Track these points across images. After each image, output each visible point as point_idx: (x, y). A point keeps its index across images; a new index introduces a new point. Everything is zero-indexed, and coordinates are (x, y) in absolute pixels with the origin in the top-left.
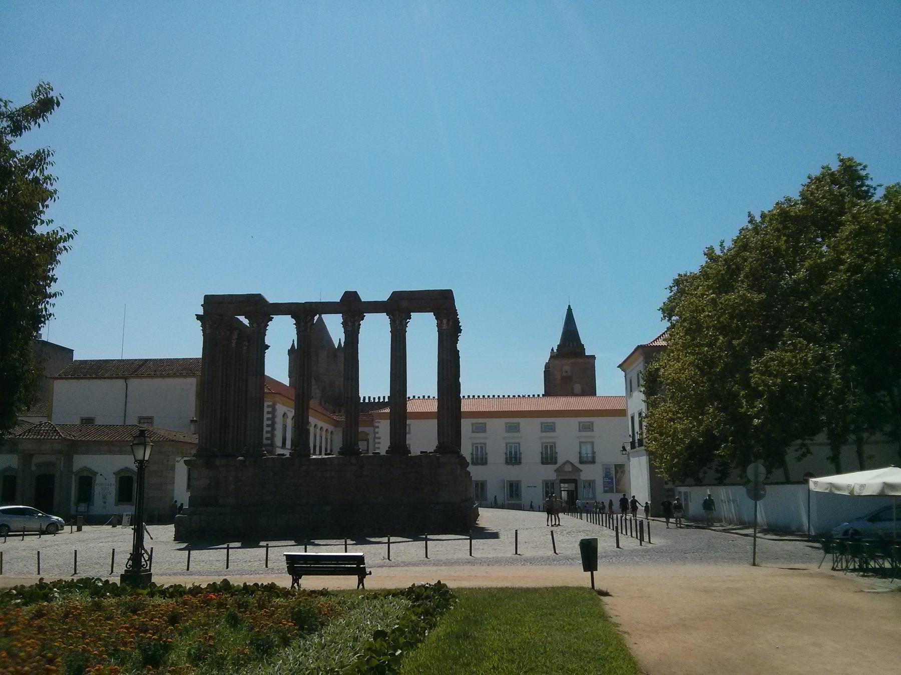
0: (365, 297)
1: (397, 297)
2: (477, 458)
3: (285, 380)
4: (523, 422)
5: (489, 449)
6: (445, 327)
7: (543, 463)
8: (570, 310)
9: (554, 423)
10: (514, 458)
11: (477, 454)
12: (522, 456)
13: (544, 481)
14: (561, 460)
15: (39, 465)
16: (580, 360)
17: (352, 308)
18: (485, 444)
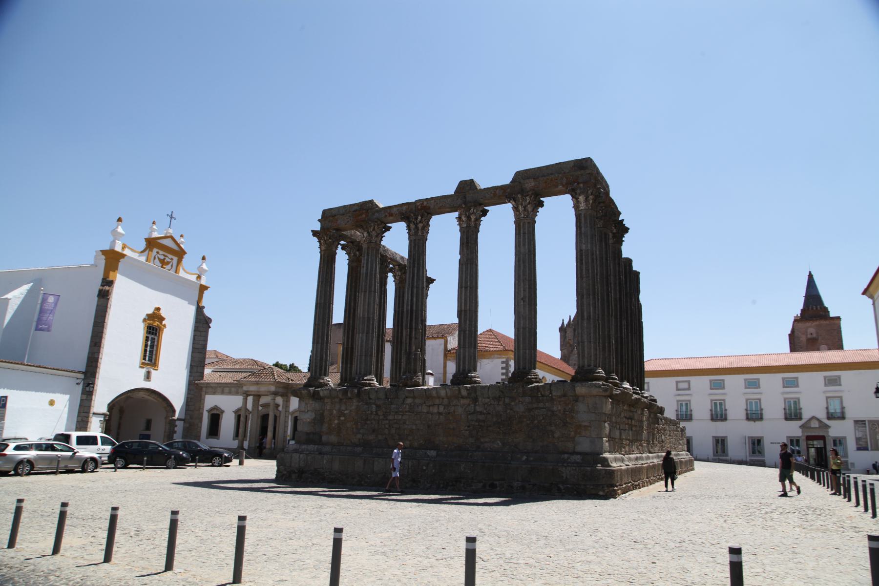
0: (483, 183)
1: (521, 177)
2: (717, 415)
3: (557, 354)
4: (763, 378)
6: (582, 206)
7: (786, 419)
8: (810, 276)
9: (797, 378)
10: (754, 415)
11: (716, 411)
12: (764, 412)
14: (806, 416)
15: (263, 406)
16: (823, 322)
17: (470, 202)
18: (724, 400)
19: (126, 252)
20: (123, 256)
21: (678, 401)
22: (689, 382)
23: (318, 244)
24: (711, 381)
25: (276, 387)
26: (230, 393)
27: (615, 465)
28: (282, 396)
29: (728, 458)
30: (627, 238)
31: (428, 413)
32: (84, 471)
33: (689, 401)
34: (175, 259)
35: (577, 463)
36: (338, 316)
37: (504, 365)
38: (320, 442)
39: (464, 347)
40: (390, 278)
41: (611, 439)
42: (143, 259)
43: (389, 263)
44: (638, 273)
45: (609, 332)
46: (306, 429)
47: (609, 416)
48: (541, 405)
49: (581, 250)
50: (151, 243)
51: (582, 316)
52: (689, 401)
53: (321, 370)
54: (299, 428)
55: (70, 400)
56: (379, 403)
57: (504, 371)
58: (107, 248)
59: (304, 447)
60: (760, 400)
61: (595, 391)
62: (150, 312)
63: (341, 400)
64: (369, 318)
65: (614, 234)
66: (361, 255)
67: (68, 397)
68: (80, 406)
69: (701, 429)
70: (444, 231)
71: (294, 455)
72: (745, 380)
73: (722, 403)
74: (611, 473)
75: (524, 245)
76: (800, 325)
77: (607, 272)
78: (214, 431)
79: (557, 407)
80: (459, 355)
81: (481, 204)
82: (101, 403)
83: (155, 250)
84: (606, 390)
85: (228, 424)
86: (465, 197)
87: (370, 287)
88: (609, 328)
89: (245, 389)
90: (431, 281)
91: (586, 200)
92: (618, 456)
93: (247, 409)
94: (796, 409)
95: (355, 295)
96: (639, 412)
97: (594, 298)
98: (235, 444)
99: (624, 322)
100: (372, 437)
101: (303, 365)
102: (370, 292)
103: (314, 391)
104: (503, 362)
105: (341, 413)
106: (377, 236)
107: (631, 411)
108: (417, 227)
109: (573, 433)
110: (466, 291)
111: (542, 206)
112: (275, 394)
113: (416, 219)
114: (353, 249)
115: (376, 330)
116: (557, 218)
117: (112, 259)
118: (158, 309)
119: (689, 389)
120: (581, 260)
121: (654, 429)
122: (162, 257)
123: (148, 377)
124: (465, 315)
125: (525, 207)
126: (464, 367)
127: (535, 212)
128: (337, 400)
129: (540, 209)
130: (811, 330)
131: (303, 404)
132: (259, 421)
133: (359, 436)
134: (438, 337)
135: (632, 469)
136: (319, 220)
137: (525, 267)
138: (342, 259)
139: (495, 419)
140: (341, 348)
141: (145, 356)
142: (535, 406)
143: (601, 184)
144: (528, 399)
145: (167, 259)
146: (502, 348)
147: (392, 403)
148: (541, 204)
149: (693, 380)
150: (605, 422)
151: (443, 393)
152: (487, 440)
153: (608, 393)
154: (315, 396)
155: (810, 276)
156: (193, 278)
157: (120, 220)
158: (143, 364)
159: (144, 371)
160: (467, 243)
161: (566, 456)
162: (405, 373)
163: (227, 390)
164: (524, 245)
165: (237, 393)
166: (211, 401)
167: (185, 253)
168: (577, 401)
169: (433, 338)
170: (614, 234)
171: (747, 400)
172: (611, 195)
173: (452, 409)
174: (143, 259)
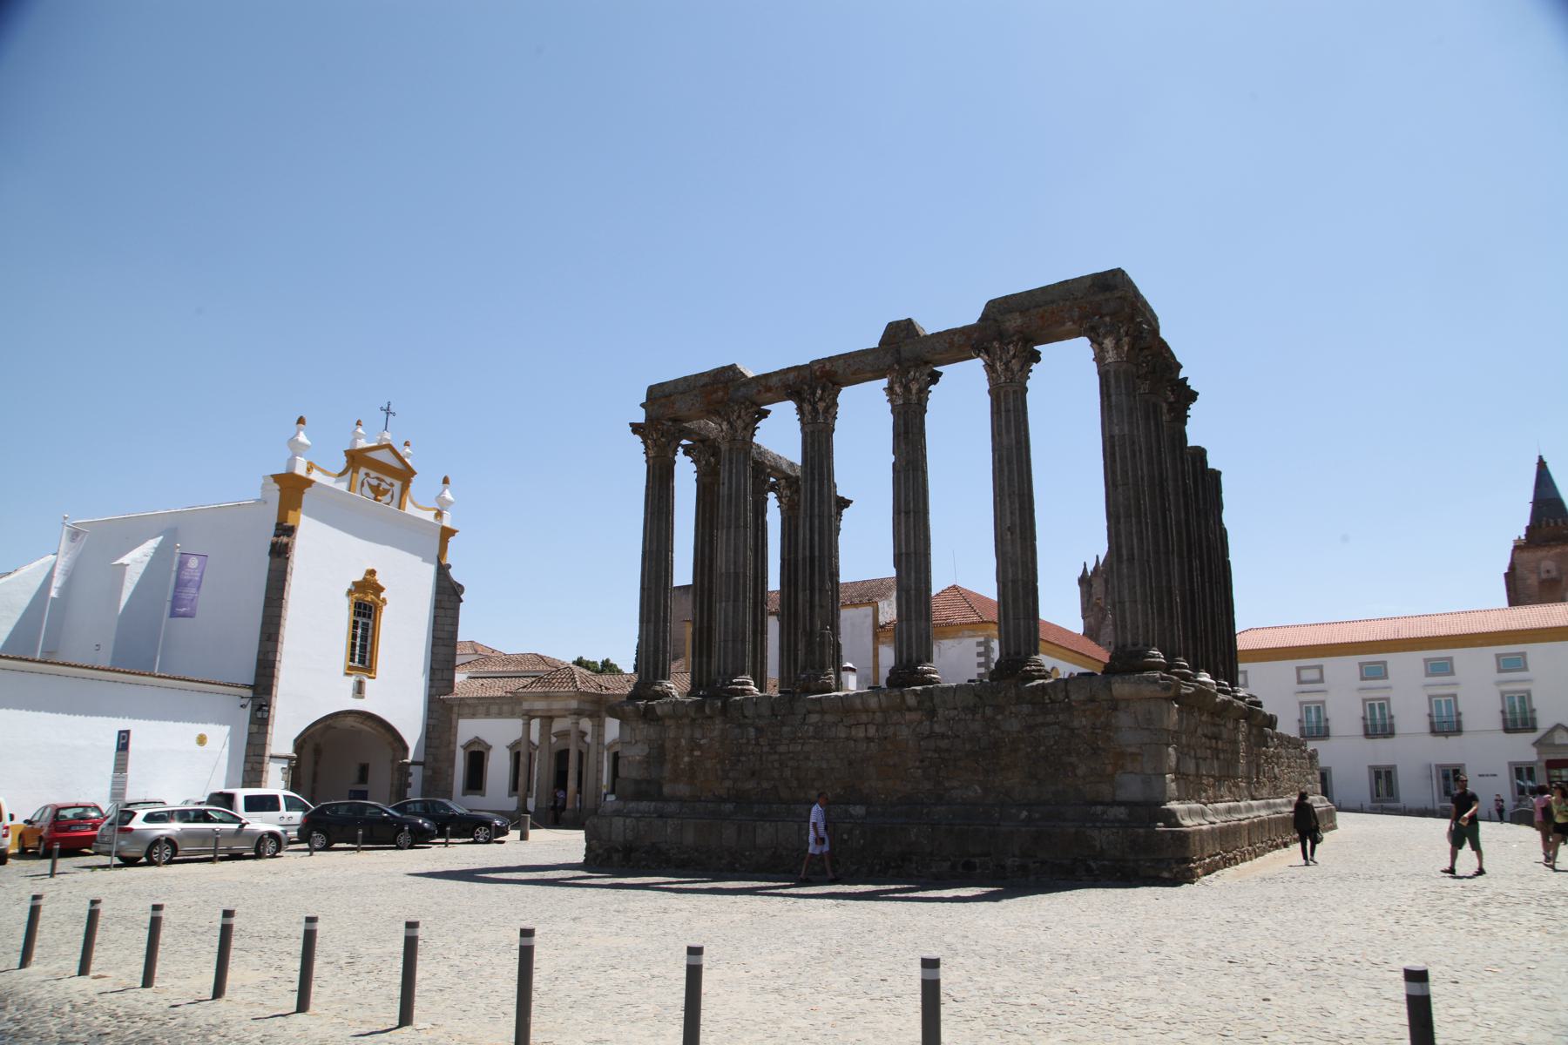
0: (930, 325)
1: (997, 310)
2: (1375, 726)
3: (1076, 625)
4: (1459, 655)
5: (1396, 708)
7: (1507, 730)
8: (1542, 465)
9: (1524, 654)
10: (1446, 725)
12: (1464, 719)
13: (1510, 764)
14: (1544, 723)
15: (557, 735)
17: (907, 360)
18: (1388, 699)
19: (315, 476)
20: (310, 483)
21: (1301, 703)
22: (1320, 668)
23: (642, 447)
24: (1361, 665)
25: (580, 702)
26: (500, 715)
27: (1189, 823)
28: (590, 716)
29: (1400, 805)
30: (1194, 410)
31: (847, 739)
32: (258, 855)
33: (1323, 702)
34: (398, 484)
35: (1120, 821)
36: (683, 572)
37: (982, 649)
38: (660, 797)
39: (909, 620)
40: (772, 502)
41: (1180, 775)
42: (343, 486)
43: (769, 475)
44: (1219, 473)
45: (1169, 581)
46: (635, 774)
47: (1176, 735)
48: (1050, 718)
49: (1112, 437)
50: (356, 459)
51: (1119, 556)
52: (1323, 702)
53: (656, 668)
54: (622, 772)
55: (231, 734)
56: (761, 723)
57: (982, 660)
58: (282, 471)
59: (632, 805)
60: (1455, 696)
61: (1147, 690)
62: (359, 577)
63: (693, 720)
64: (736, 574)
65: (1171, 404)
66: (718, 463)
67: (227, 729)
68: (249, 743)
69: (1347, 754)
70: (864, 413)
71: (615, 819)
72: (1426, 661)
73: (1384, 705)
74: (1183, 838)
75: (1008, 432)
76: (1526, 555)
77: (1161, 474)
78: (476, 779)
79: (1081, 722)
80: (900, 633)
81: (927, 363)
82: (282, 739)
83: (363, 471)
84: (1167, 688)
85: (498, 768)
86: (898, 352)
87: (737, 519)
88: (1168, 574)
89: (526, 706)
90: (845, 503)
91: (1117, 345)
92: (1195, 806)
93: (530, 742)
94: (1524, 711)
95: (711, 536)
96: (1230, 725)
97: (1139, 522)
98: (512, 804)
99: (1196, 563)
100: (750, 785)
101: (626, 662)
102: (737, 527)
103: (646, 706)
104: (979, 644)
105: (694, 745)
106: (745, 429)
107: (1215, 725)
108: (815, 410)
109: (1110, 768)
110: (908, 518)
111: (1038, 360)
112: (579, 713)
113: (814, 394)
114: (704, 452)
115: (750, 595)
116: (1067, 380)
117: (292, 489)
118: (372, 572)
119: (1321, 680)
120: (1113, 454)
121: (1258, 756)
122: (375, 482)
123: (359, 690)
124: (908, 561)
125: (1006, 364)
126: (909, 654)
127: (1025, 372)
128: (686, 721)
129: (1034, 366)
130: (1548, 564)
131: (628, 730)
132: (553, 762)
133: (728, 783)
134: (861, 604)
135: (1221, 829)
136: (642, 405)
137: (1010, 471)
138: (685, 473)
139: (968, 747)
140: (689, 629)
141: (353, 654)
142: (1040, 720)
143: (1144, 315)
144: (1026, 709)
145: (384, 486)
146: (976, 619)
147: (783, 724)
148: (1036, 357)
149: (1328, 663)
150: (1168, 745)
151: (873, 702)
152: (956, 784)
153: (1171, 693)
154: (648, 716)
155: (1542, 465)
156: (429, 516)
157: (301, 421)
158: (350, 668)
159: (352, 680)
160: (906, 432)
161: (1099, 808)
162: (804, 669)
163: (494, 709)
164: (1008, 432)
165: (512, 715)
166: (468, 729)
167: (414, 473)
168: (1115, 709)
169: (853, 605)
170: (1171, 404)
171: (1430, 698)
172: (1163, 334)
173: (890, 731)
174: (343, 486)
